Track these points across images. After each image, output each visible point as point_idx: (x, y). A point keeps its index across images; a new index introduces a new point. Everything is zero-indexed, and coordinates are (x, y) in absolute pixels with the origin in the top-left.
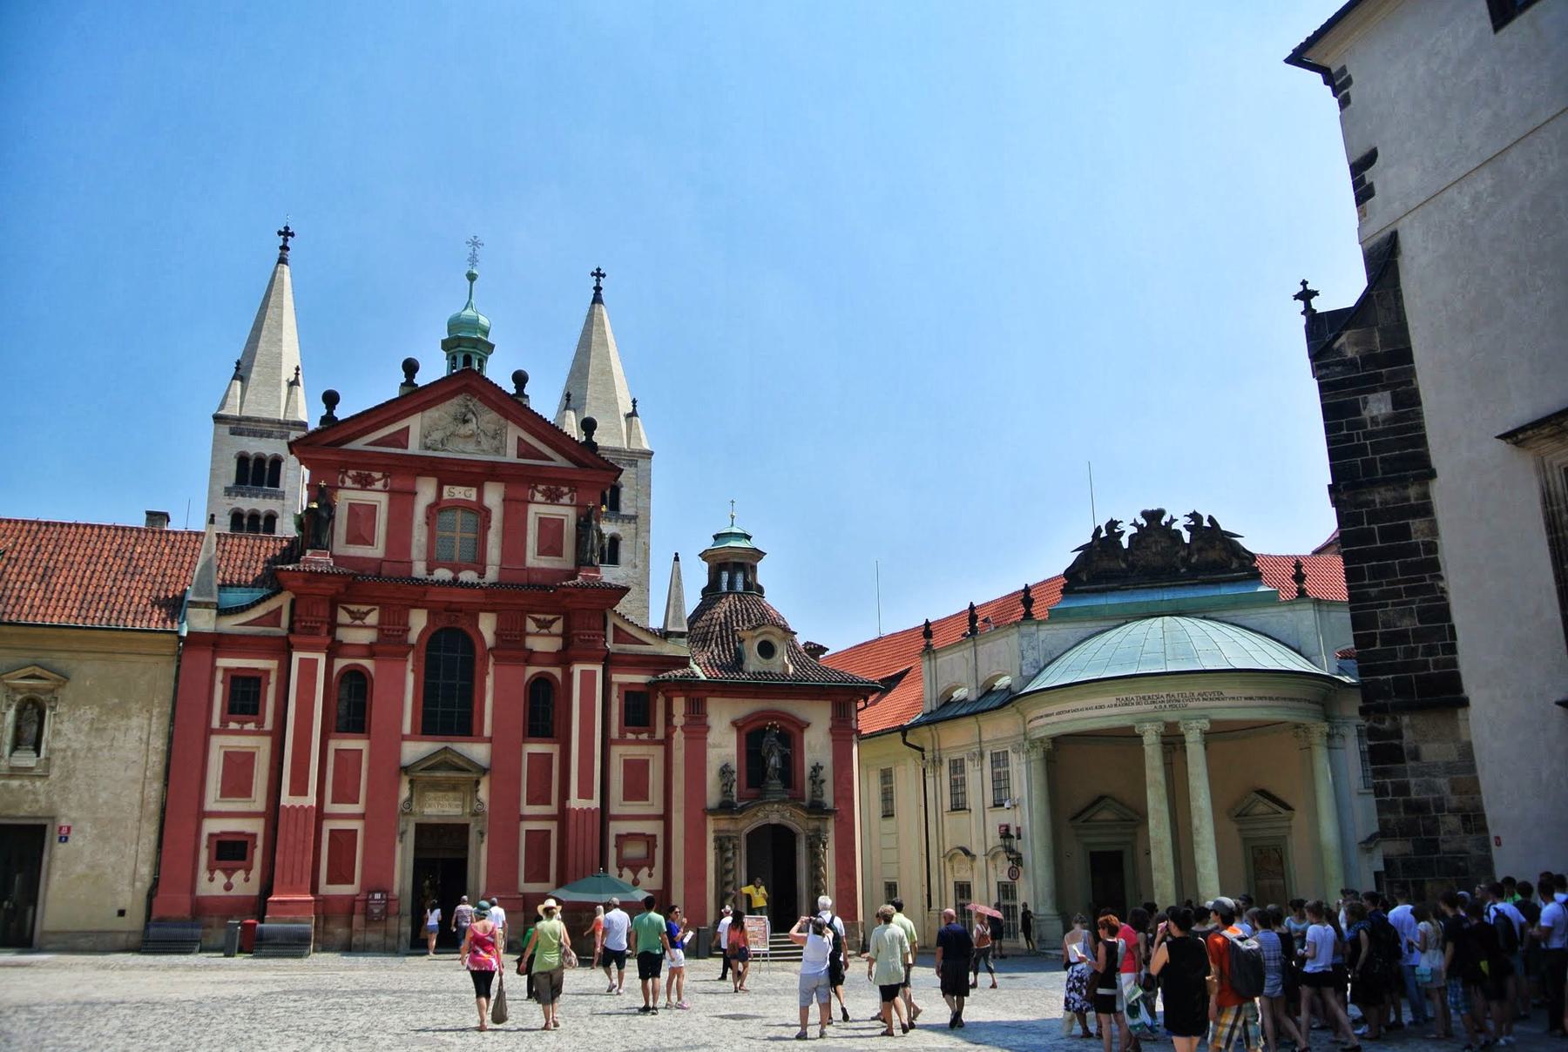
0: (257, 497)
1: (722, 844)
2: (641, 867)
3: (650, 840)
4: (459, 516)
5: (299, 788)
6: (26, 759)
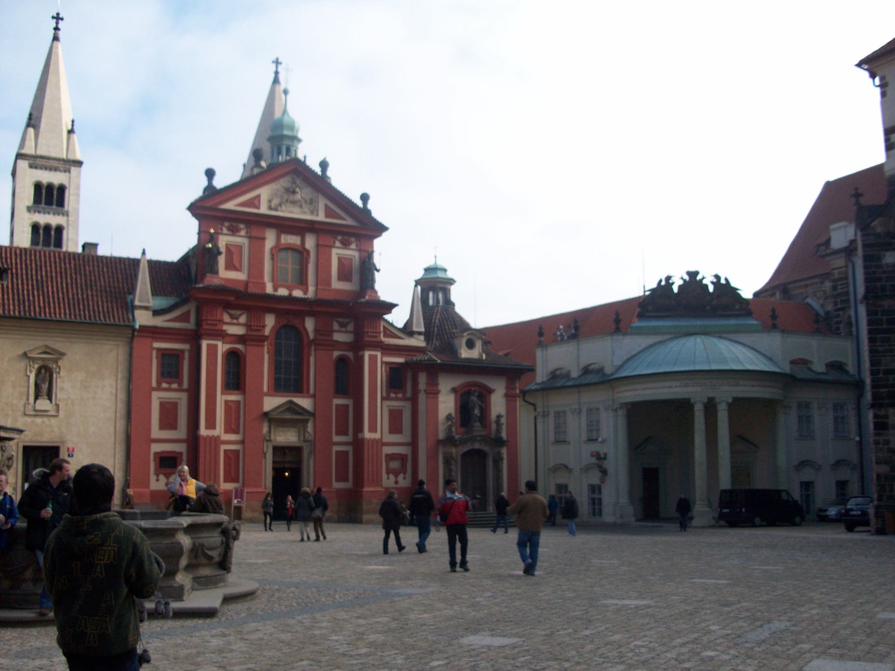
0: (49, 213)
1: (448, 461)
2: (399, 473)
3: (402, 458)
4: (290, 255)
5: (211, 425)
6: (43, 404)
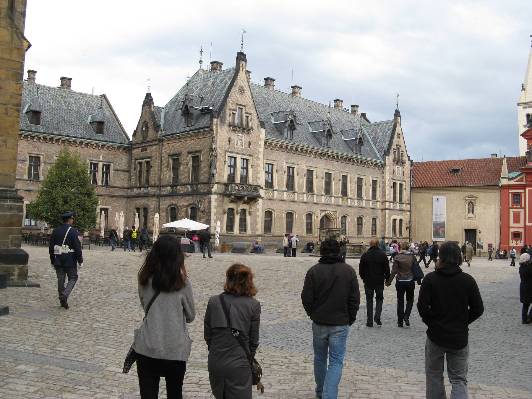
6: (471, 215)
